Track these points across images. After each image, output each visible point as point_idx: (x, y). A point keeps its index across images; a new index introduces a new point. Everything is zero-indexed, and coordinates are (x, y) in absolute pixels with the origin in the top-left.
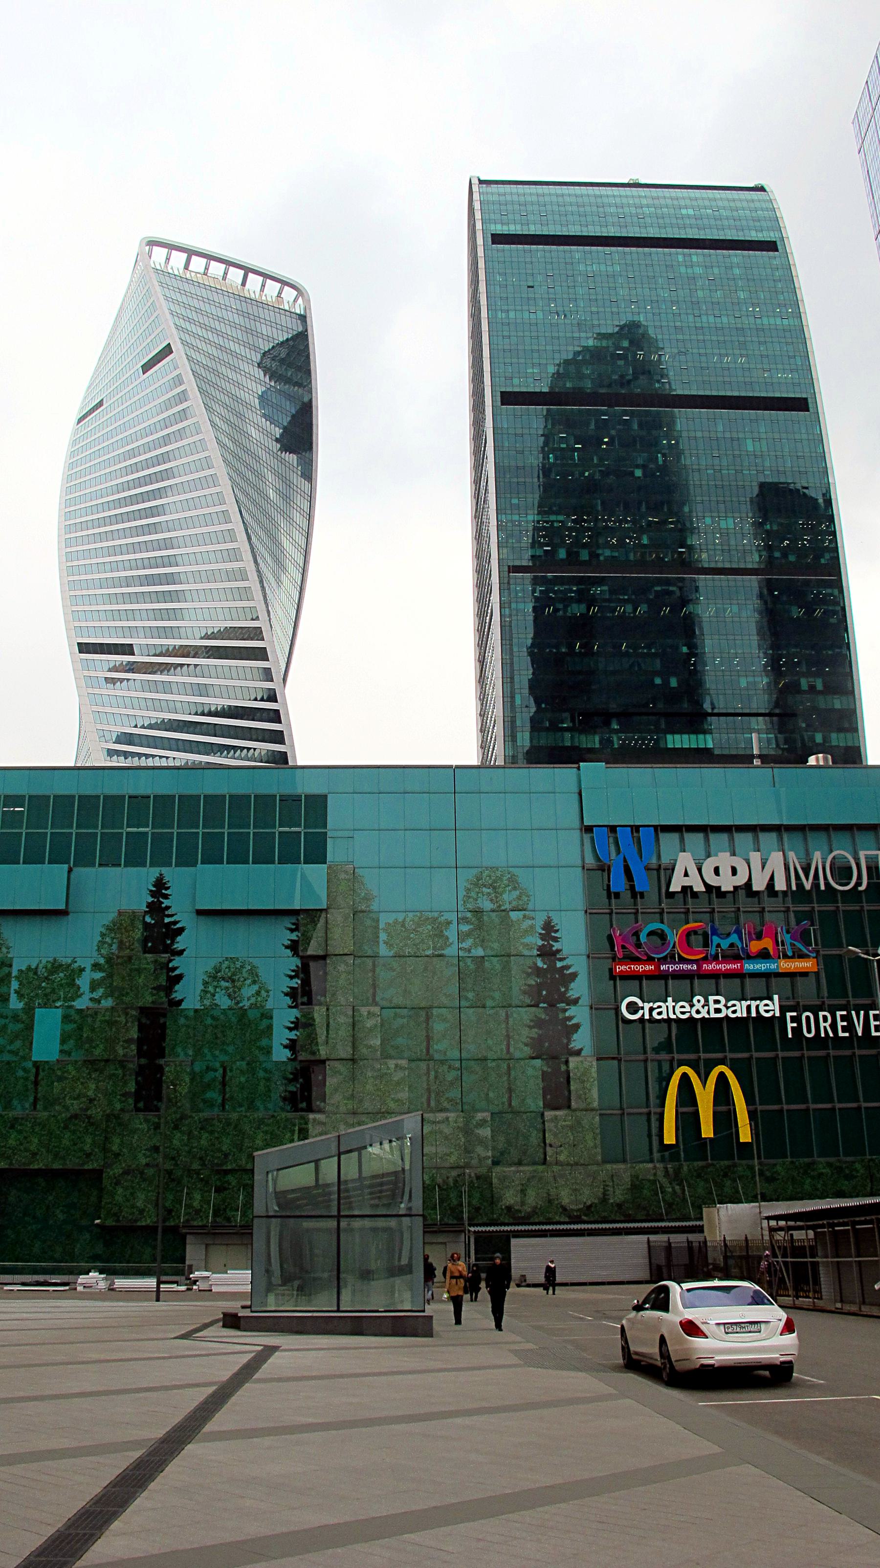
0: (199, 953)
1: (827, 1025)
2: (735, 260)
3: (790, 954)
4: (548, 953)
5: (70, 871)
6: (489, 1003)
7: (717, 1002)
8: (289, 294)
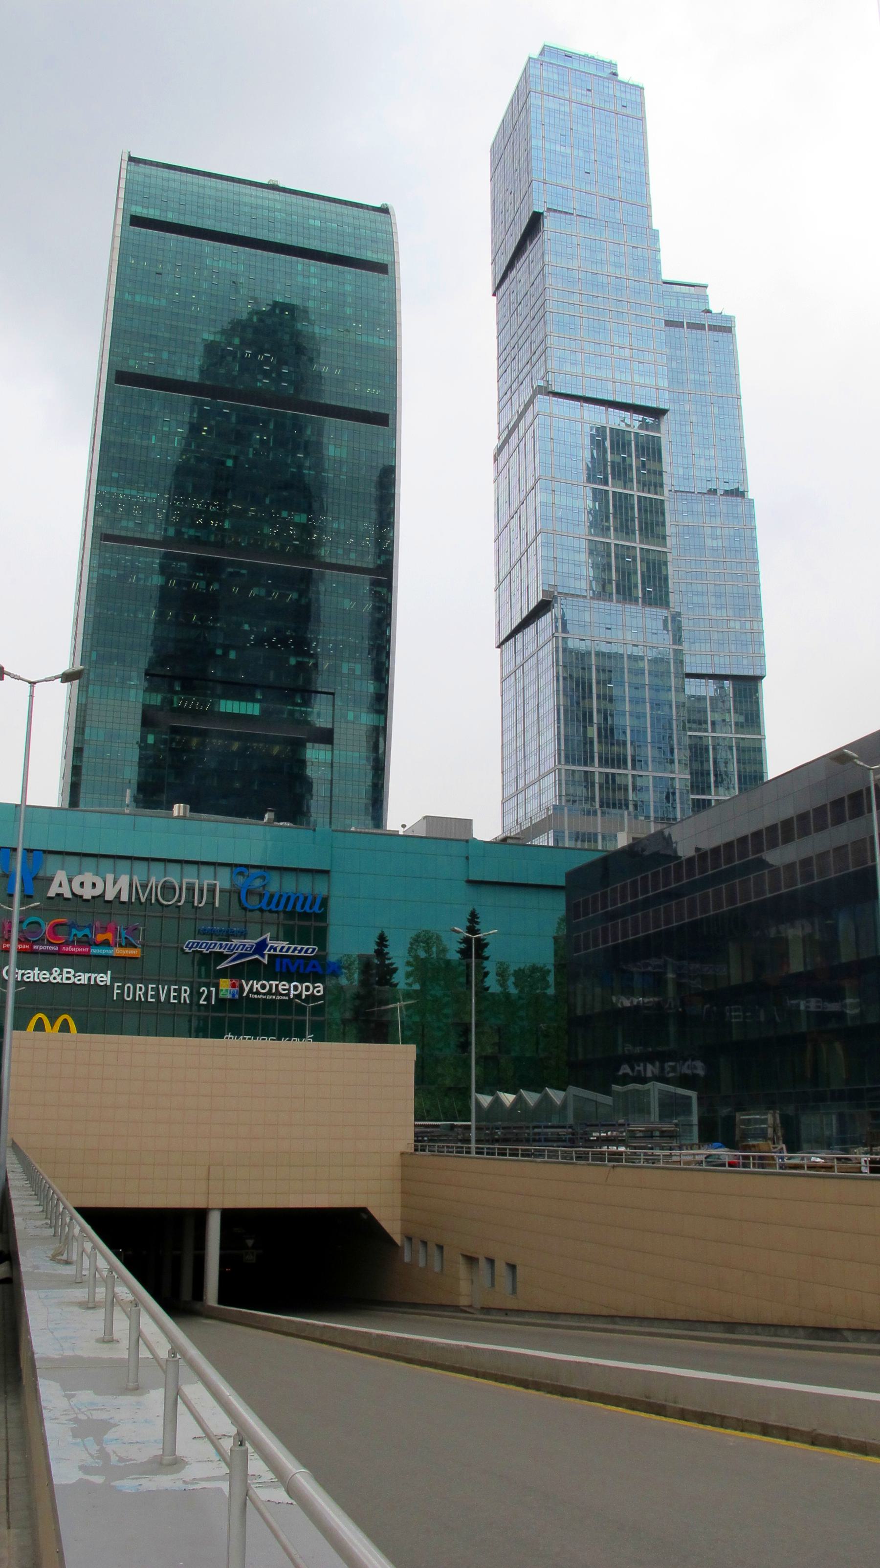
1: (141, 993)
2: (349, 277)
3: (124, 944)
7: (68, 973)
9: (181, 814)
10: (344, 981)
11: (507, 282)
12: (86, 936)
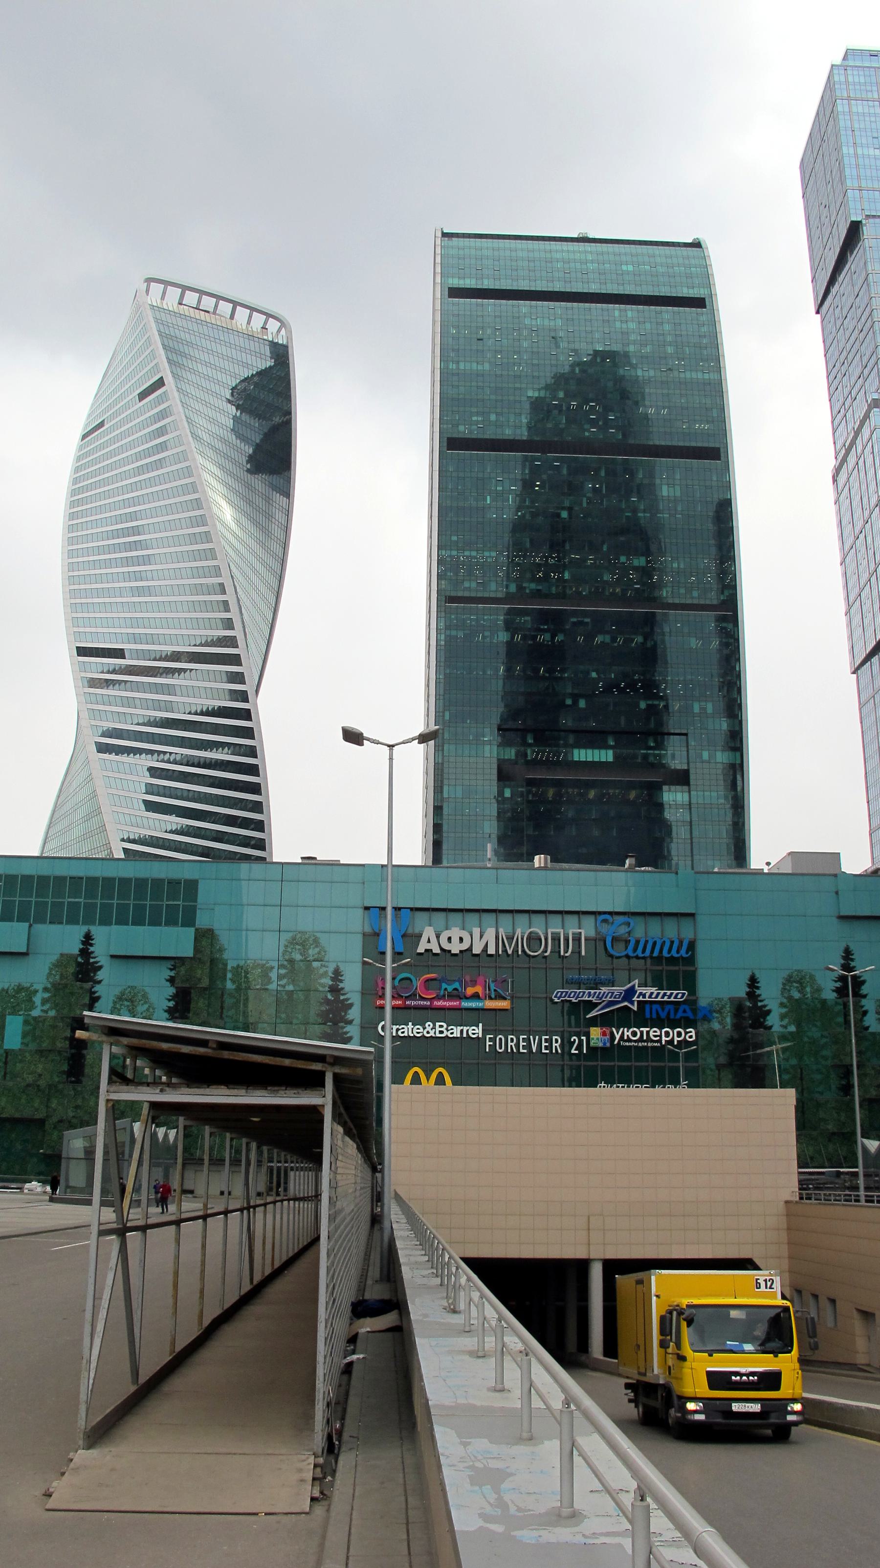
0: (110, 980)
3: (493, 996)
4: (335, 990)
5: (30, 926)
6: (295, 1021)
7: (441, 1026)
8: (273, 326)
9: (542, 865)
10: (716, 1026)
11: (830, 298)
12: (456, 989)
